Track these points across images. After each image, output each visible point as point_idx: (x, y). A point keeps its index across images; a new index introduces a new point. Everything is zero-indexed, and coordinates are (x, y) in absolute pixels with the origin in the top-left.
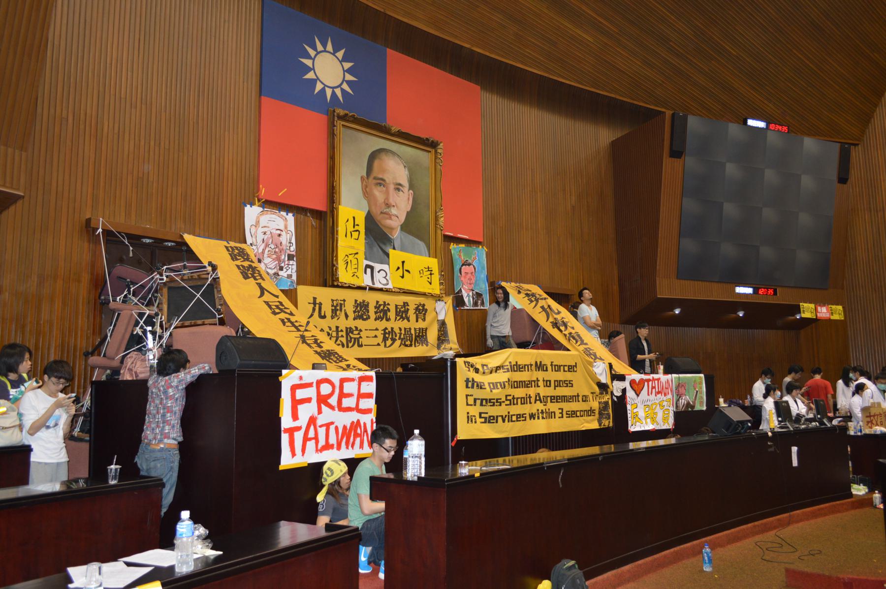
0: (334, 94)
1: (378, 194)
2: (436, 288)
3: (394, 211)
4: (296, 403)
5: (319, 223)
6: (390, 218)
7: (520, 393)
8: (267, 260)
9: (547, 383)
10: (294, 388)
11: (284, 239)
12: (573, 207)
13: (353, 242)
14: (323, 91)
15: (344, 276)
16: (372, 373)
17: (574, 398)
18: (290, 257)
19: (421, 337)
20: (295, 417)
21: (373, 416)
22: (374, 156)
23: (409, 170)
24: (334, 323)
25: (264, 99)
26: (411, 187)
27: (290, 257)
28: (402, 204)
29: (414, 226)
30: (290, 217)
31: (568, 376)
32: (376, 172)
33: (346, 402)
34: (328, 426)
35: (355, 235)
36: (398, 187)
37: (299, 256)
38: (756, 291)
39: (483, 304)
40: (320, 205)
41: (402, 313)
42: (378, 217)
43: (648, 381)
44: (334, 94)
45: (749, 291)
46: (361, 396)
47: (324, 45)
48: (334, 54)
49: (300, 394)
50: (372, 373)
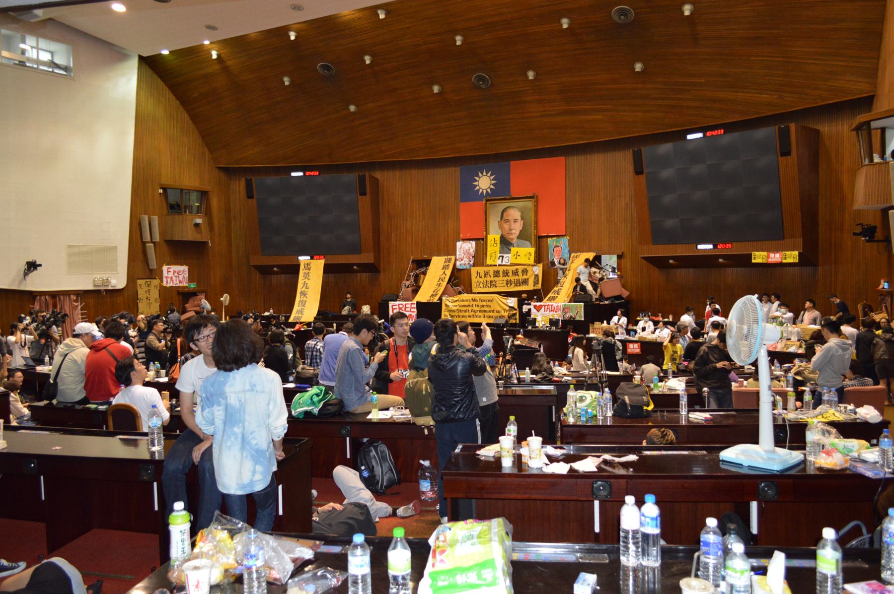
1: (506, 226)
2: (532, 262)
5: (481, 242)
6: (511, 234)
12: (627, 204)
13: (493, 248)
15: (489, 261)
19: (525, 282)
26: (522, 218)
28: (517, 228)
29: (523, 236)
31: (489, 303)
32: (505, 217)
38: (715, 246)
41: (515, 273)
42: (506, 236)
45: (710, 246)
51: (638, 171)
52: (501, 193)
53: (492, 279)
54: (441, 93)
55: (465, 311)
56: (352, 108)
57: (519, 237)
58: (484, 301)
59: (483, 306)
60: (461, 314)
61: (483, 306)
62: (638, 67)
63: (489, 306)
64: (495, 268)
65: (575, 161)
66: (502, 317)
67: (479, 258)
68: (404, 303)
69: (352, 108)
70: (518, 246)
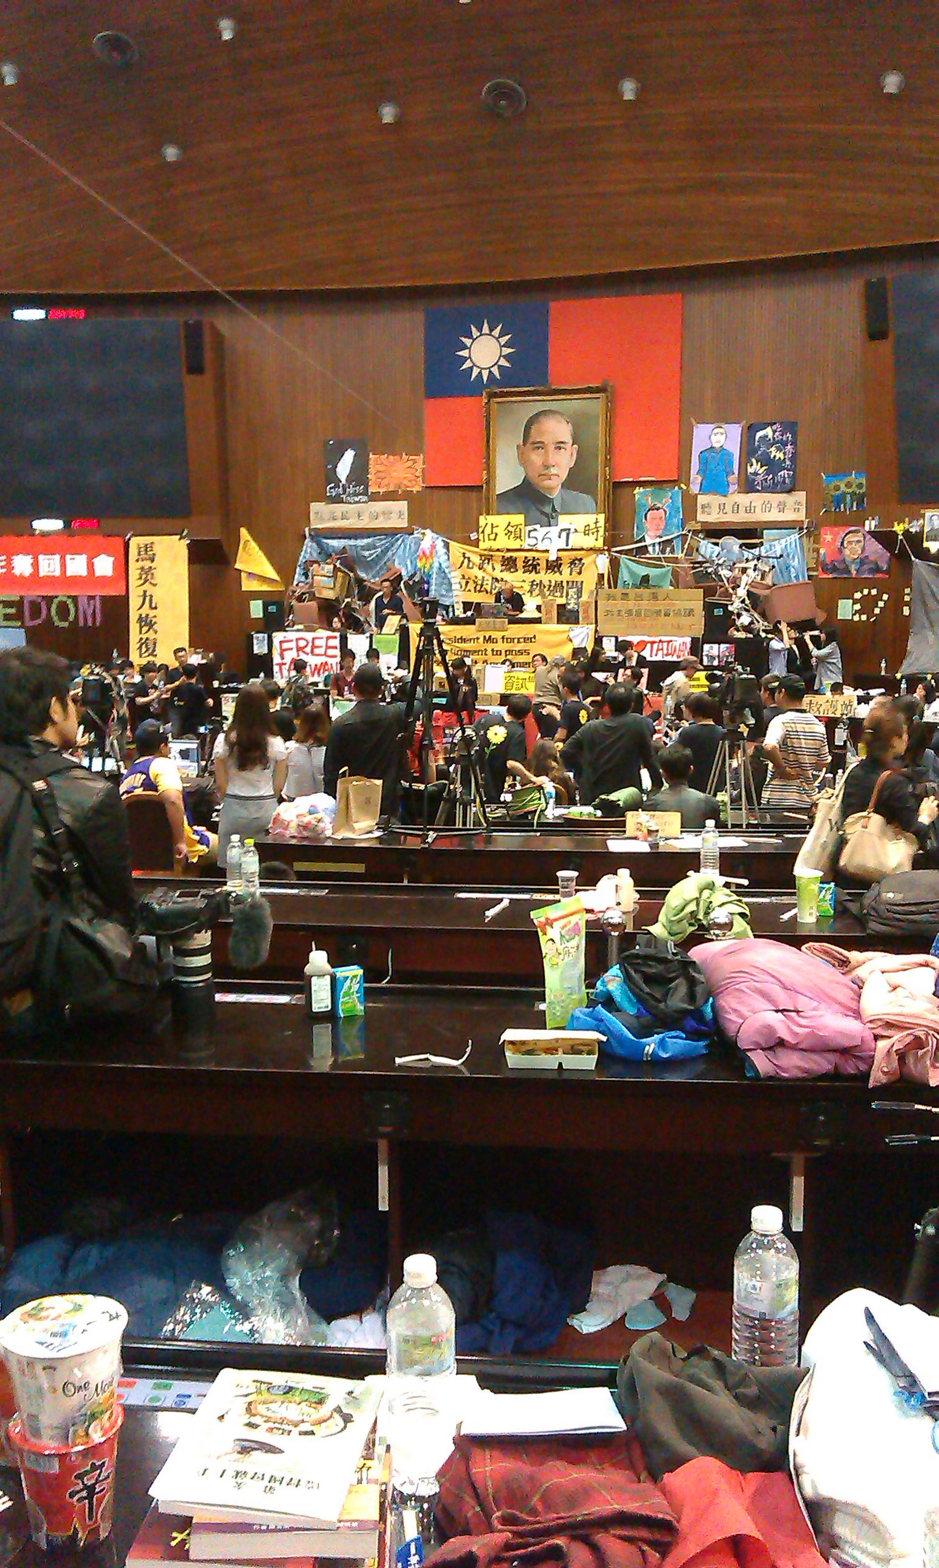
1: (536, 458)
3: (553, 471)
4: (282, 651)
10: (281, 642)
21: (338, 659)
23: (573, 426)
28: (563, 462)
29: (576, 481)
32: (534, 436)
36: (559, 446)
43: (653, 643)
46: (328, 647)
47: (480, 329)
48: (490, 335)
49: (285, 646)
50: (337, 634)
51: (876, 333)
54: (399, 123)
56: (171, 153)
57: (568, 485)
62: (892, 83)
65: (707, 306)
68: (309, 636)
69: (171, 153)
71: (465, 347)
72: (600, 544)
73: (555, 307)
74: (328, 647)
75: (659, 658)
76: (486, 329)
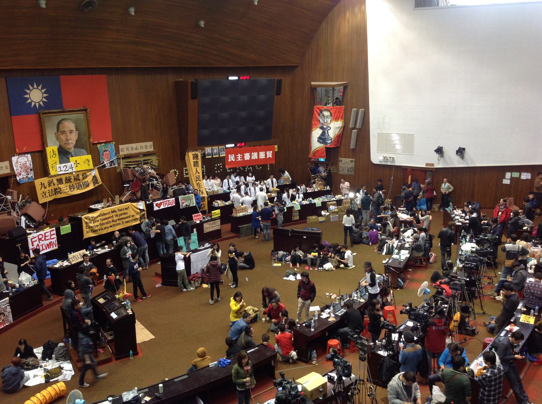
0: (39, 104)
1: (63, 137)
2: (91, 167)
3: (70, 141)
4: (32, 243)
6: (69, 144)
7: (104, 222)
8: (23, 173)
9: (117, 216)
10: (31, 240)
11: (28, 164)
13: (54, 159)
14: (35, 105)
15: (52, 172)
16: (54, 228)
17: (127, 217)
18: (31, 170)
20: (33, 245)
22: (59, 123)
24: (50, 188)
25: (12, 117)
26: (77, 129)
27: (31, 170)
28: (73, 138)
30: (29, 156)
31: (125, 211)
32: (61, 129)
33: (47, 238)
34: (42, 245)
35: (54, 156)
36: (71, 132)
37: (34, 169)
39: (114, 164)
40: (40, 149)
41: (77, 179)
42: (64, 146)
44: (39, 104)
46: (51, 235)
47: (33, 86)
49: (33, 240)
50: (54, 228)
52: (54, 104)
53: (56, 187)
55: (107, 223)
57: (76, 146)
58: (121, 210)
59: (121, 215)
60: (103, 227)
61: (121, 215)
63: (125, 214)
64: (59, 177)
66: (137, 219)
67: (42, 168)
68: (42, 232)
70: (76, 156)
71: (27, 94)
72: (92, 167)
73: (63, 78)
74: (51, 235)
75: (166, 207)
76: (35, 86)
